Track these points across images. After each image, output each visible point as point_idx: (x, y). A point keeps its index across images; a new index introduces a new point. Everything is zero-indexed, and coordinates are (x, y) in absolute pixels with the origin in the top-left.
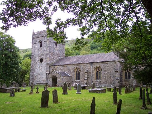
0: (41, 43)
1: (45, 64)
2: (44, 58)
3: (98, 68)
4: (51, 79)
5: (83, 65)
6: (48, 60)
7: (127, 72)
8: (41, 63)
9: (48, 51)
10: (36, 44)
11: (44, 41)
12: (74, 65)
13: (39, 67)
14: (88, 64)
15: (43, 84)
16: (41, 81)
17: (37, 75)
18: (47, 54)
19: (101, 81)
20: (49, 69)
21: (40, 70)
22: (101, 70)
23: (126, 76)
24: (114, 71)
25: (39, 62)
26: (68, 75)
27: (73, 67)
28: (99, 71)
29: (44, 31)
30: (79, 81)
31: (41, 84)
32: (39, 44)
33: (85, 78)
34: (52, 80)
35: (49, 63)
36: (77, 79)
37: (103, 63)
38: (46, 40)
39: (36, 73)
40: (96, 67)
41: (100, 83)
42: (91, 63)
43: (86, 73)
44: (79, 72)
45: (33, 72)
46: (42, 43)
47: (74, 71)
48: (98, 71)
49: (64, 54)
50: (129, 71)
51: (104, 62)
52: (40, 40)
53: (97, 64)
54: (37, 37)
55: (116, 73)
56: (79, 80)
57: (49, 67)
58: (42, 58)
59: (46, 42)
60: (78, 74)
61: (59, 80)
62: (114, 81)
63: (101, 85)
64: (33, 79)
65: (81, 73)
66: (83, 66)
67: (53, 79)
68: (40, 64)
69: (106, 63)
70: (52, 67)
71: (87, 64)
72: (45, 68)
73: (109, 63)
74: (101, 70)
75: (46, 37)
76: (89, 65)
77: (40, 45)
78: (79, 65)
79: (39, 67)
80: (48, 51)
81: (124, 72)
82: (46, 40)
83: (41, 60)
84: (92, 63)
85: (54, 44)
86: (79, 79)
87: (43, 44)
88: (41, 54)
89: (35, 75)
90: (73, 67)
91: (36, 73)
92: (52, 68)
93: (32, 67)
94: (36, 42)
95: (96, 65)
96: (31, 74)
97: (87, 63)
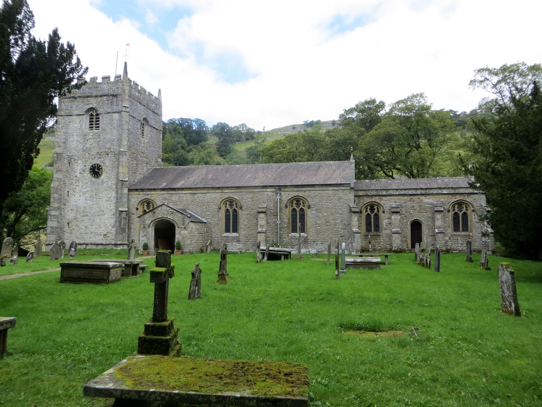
0: (95, 117)
1: (112, 183)
2: (107, 164)
3: (297, 200)
4: (151, 232)
5: (250, 190)
6: (123, 170)
7: (372, 216)
8: (94, 179)
9: (125, 143)
10: (76, 117)
11: (109, 110)
12: (219, 191)
13: (84, 193)
14: (268, 190)
15: (102, 244)
16: (92, 235)
17: (75, 218)
18: (120, 153)
19: (306, 237)
20: (126, 200)
21: (91, 203)
22: (309, 207)
23: (368, 224)
24: (346, 210)
25: (88, 175)
26: (199, 217)
27: (217, 197)
28: (302, 209)
29: (108, 78)
30: (239, 237)
31: (94, 247)
32: (86, 119)
33: (260, 229)
34: (153, 234)
35: (127, 179)
36: (227, 230)
37: (311, 189)
38: (115, 108)
39: (72, 210)
40: (291, 201)
41: (306, 241)
42: (278, 186)
43: (262, 215)
44: (235, 211)
45: (59, 208)
46: (97, 115)
47: (220, 208)
48: (296, 208)
49: (159, 157)
50: (376, 211)
51: (317, 185)
52: (91, 106)
53: (296, 189)
54: (80, 97)
55: (353, 215)
56: (235, 234)
57: (129, 194)
58: (97, 161)
59: (116, 116)
60: (231, 214)
61: (182, 232)
62: (347, 236)
63: (306, 247)
64: (59, 231)
65: (243, 216)
66: (251, 195)
67: (157, 231)
68: (89, 183)
69: (324, 188)
70: (137, 193)
71: (264, 190)
72: (113, 194)
73: (331, 188)
74: (309, 207)
75: (115, 99)
76: (269, 192)
77: (88, 123)
78: (238, 191)
79: (84, 193)
80: (125, 143)
81: (364, 214)
82: (115, 107)
83: (96, 171)
84: (280, 188)
85: (139, 126)
86: (235, 230)
87: (104, 120)
88: (94, 152)
89: (70, 215)
90: (217, 197)
91: (72, 210)
92: (137, 198)
93: (57, 190)
94: (76, 112)
95: (292, 193)
96: (53, 213)
97: (265, 187)
